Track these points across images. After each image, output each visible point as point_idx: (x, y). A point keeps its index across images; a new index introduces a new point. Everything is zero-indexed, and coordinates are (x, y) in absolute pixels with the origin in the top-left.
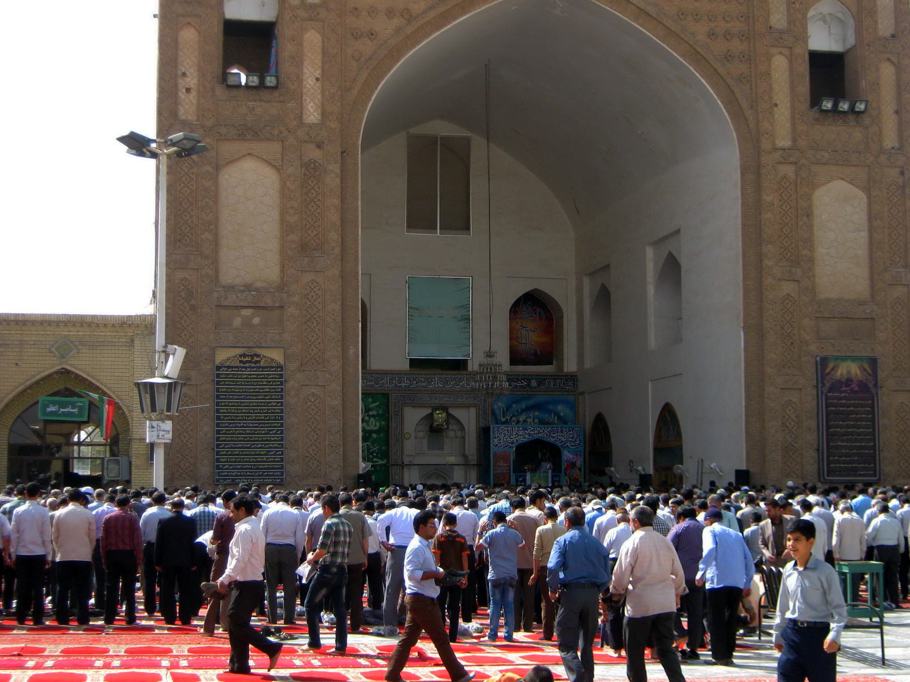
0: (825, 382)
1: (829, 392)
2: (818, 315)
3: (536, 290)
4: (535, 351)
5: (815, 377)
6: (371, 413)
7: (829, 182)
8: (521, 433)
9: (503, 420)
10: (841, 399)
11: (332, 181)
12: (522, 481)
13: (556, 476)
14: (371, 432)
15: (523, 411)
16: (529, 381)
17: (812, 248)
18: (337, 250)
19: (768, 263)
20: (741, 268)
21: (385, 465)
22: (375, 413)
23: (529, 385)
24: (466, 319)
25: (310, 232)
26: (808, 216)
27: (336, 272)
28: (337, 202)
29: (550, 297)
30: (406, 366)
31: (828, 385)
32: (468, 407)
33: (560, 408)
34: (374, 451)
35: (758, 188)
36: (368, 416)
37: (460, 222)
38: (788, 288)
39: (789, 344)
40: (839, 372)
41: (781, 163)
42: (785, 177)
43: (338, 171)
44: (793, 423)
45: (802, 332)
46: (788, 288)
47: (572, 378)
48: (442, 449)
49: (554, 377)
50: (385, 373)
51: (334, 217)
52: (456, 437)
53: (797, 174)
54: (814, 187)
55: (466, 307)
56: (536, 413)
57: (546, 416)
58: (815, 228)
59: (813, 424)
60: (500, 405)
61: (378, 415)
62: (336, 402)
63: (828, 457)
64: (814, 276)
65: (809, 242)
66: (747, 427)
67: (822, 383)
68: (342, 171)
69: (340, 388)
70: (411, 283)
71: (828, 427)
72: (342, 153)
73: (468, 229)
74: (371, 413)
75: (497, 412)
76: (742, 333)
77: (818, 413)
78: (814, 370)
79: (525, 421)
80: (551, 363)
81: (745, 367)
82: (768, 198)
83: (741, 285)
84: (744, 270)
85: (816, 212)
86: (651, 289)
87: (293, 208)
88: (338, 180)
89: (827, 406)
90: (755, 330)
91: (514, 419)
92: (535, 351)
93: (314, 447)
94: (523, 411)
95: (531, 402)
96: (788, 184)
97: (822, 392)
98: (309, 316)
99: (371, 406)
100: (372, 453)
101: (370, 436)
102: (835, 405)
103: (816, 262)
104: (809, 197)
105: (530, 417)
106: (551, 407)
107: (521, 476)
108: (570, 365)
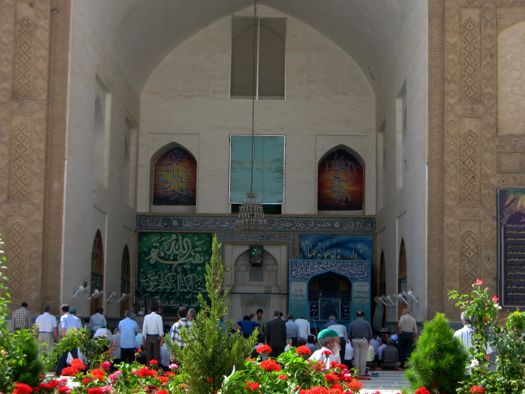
0: (505, 214)
1: (508, 223)
2: (500, 150)
3: (342, 145)
4: (347, 198)
5: (495, 209)
6: (196, 249)
7: (514, 24)
8: (315, 267)
9: (310, 256)
10: (520, 230)
11: (42, 35)
12: (315, 308)
13: (345, 304)
14: (197, 265)
15: (327, 248)
16: (333, 223)
17: (496, 87)
18: (44, 96)
19: (450, 100)
20: (427, 107)
22: (200, 249)
23: (332, 226)
24: (280, 171)
25: (21, 81)
26: (491, 56)
27: (42, 115)
28: (44, 53)
29: (355, 152)
30: (230, 211)
31: (507, 217)
32: (280, 244)
33: (360, 246)
34: (199, 282)
35: (443, 32)
36: (195, 252)
37: (275, 89)
38: (470, 125)
39: (469, 178)
40: (519, 204)
41: (465, 7)
42: (469, 21)
43: (47, 27)
44: (472, 254)
45: (483, 166)
46: (470, 125)
47: (371, 221)
48: (262, 280)
49: (358, 218)
50: (210, 216)
51: (43, 66)
52: (274, 271)
53: (481, 16)
54: (498, 28)
55: (280, 160)
56: (339, 251)
57: (347, 253)
58: (499, 67)
59: (492, 253)
60: (307, 243)
61: (202, 251)
62: (38, 230)
63: (506, 286)
64: (497, 113)
65: (493, 81)
66: (428, 257)
67: (502, 214)
68: (51, 27)
69: (41, 219)
70: (234, 141)
71: (506, 258)
72: (52, 10)
73: (283, 95)
74: (196, 249)
75: (305, 249)
76: (427, 168)
77: (497, 244)
78: (494, 202)
79: (329, 257)
80: (361, 209)
81: (428, 200)
82: (452, 39)
83: (427, 122)
84: (430, 109)
85: (501, 53)
86: (399, 137)
87: (6, 59)
88: (47, 35)
89: (506, 237)
90: (438, 165)
91: (319, 255)
92: (347, 198)
93: (16, 271)
94: (327, 248)
95: (335, 241)
96: (472, 27)
97: (501, 224)
98: (17, 155)
100: (197, 283)
101: (196, 268)
102: (514, 236)
103: (500, 99)
104: (494, 38)
105: (333, 254)
106: (352, 245)
107: (314, 304)
108: (370, 208)
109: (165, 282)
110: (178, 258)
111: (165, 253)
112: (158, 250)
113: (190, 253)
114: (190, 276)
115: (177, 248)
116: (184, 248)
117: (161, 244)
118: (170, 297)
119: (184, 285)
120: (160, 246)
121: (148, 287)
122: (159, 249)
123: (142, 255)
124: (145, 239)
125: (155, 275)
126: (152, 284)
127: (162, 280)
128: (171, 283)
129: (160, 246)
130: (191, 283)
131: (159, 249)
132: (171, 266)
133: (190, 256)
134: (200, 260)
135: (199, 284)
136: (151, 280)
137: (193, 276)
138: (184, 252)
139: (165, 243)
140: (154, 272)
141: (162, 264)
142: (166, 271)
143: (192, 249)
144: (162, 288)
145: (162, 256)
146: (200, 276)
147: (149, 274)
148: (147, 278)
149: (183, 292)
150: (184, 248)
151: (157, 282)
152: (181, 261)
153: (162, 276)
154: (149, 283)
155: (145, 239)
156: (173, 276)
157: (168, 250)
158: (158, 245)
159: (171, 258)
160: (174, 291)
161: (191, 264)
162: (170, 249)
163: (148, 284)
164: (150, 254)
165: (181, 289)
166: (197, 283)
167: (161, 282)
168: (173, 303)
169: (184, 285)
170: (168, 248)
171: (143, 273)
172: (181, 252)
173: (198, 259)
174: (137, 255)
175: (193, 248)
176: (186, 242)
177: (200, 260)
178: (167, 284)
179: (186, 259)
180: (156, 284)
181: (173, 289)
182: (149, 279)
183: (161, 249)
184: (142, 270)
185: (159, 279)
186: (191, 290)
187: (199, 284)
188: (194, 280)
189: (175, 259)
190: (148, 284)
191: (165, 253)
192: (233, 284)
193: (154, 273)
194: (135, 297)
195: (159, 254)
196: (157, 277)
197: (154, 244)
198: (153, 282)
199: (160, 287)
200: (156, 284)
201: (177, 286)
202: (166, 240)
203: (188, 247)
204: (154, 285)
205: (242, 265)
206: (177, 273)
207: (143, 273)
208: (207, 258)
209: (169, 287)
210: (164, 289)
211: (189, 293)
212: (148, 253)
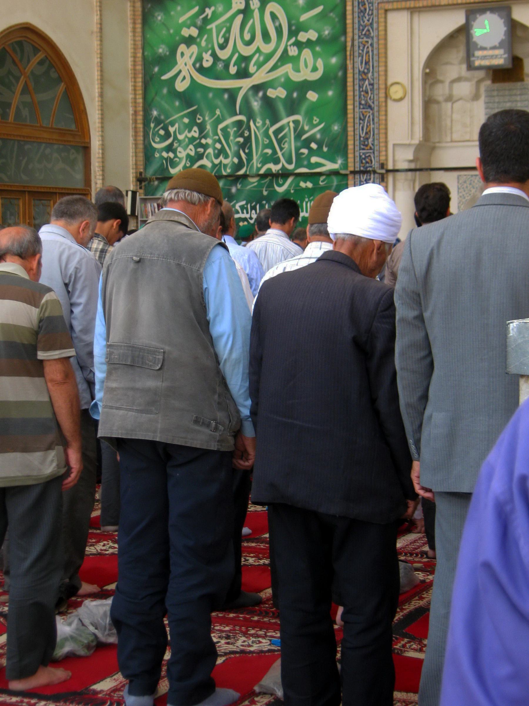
6: (303, 37)
14: (304, 86)
21: (335, 173)
22: (313, 35)
34: (311, 139)
36: (299, 45)
61: (320, 41)
74: (303, 37)
99: (304, 17)
100: (307, 144)
101: (303, 97)
109: (218, 146)
110: (252, 69)
111: (214, 55)
112: (194, 49)
113: (285, 51)
114: (284, 121)
115: (247, 37)
116: (266, 36)
117: (202, 30)
118: (234, 190)
119: (269, 151)
120: (200, 35)
121: (173, 163)
122: (199, 45)
123: (152, 68)
124: (160, 17)
125: (189, 127)
126: (182, 153)
127: (209, 141)
128: (234, 148)
129: (200, 35)
130: (291, 144)
131: (199, 45)
132: (232, 94)
133: (285, 58)
134: (315, 69)
135: (314, 146)
136: (179, 141)
137: (296, 122)
138: (267, 49)
139: (213, 26)
140: (185, 116)
141: (207, 89)
142: (218, 112)
143: (289, 39)
144: (209, 165)
145: (206, 65)
146: (316, 120)
147: (172, 124)
148: (168, 134)
149: (269, 174)
150: (266, 36)
151: (196, 147)
152: (259, 77)
153: (208, 127)
154: (174, 152)
155: (160, 17)
156: (239, 124)
157: (222, 47)
158: (194, 32)
159: (233, 70)
160: (241, 172)
161: (289, 85)
162: (227, 41)
163: (171, 155)
164: (176, 63)
165: (264, 163)
166: (307, 144)
167: (205, 147)
168: (242, 207)
169: (269, 151)
170: (221, 41)
171: (158, 122)
172: (258, 50)
173: (310, 67)
174: (139, 68)
175: (293, 33)
176: (274, 17)
177: (315, 69)
178: (221, 152)
179: (274, 68)
180: (192, 153)
181: (240, 165)
182: (175, 138)
183: (203, 44)
184: (155, 113)
185: (201, 139)
186: (291, 167)
187: (314, 146)
188: (299, 135)
189: (243, 74)
190: (171, 155)
191: (214, 55)
192: (416, 141)
193: (186, 120)
194: (130, 194)
195: (199, 59)
196: (195, 133)
197: (186, 32)
198: (185, 150)
199: (205, 162)
200: (192, 153)
201: (249, 156)
202: (215, 16)
203: (279, 30)
204: (188, 156)
205: (459, 79)
206: (251, 116)
207: (158, 122)
208: (334, 60)
209: (230, 161)
210: (214, 166)
211: (284, 175)
212: (168, 61)
